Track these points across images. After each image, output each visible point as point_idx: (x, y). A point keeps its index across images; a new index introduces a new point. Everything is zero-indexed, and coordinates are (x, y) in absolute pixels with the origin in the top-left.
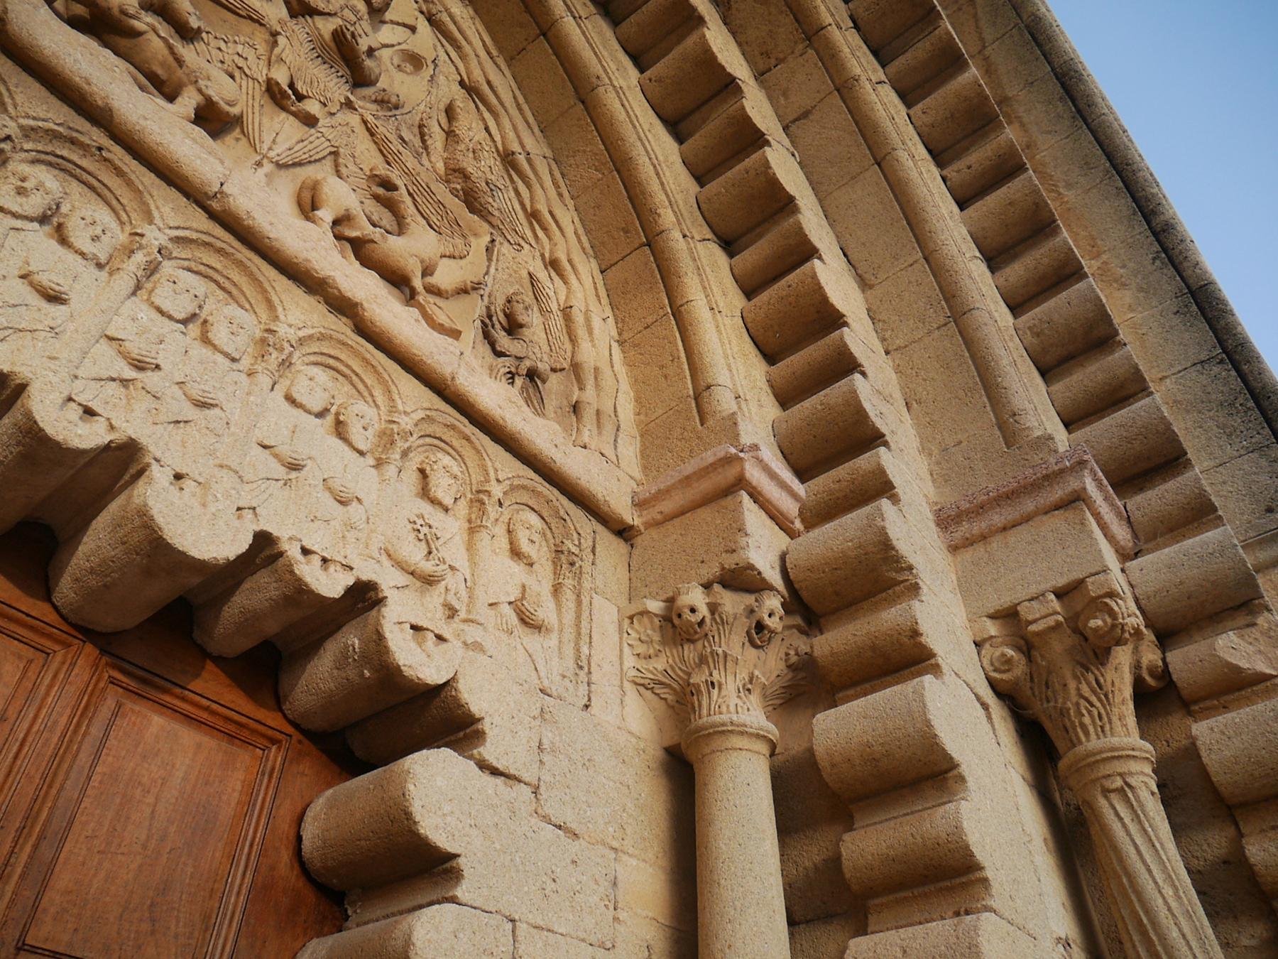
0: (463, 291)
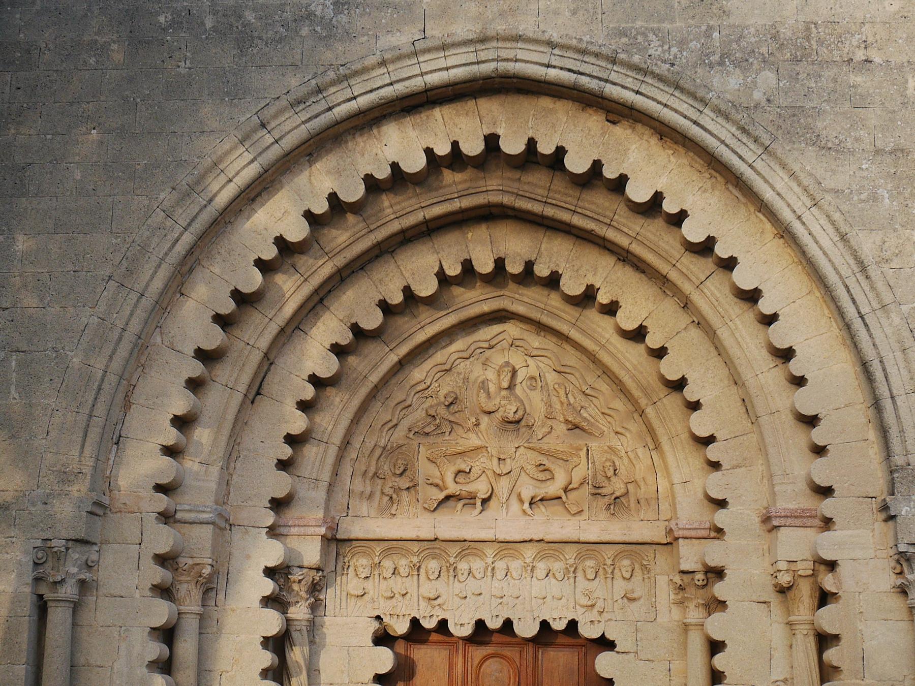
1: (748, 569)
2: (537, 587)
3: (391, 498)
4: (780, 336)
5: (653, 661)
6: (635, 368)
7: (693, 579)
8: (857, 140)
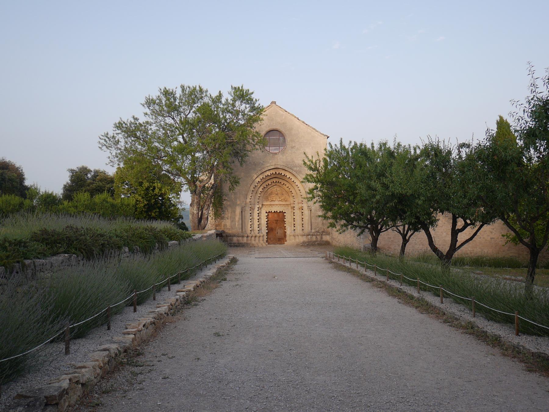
1: (297, 207)
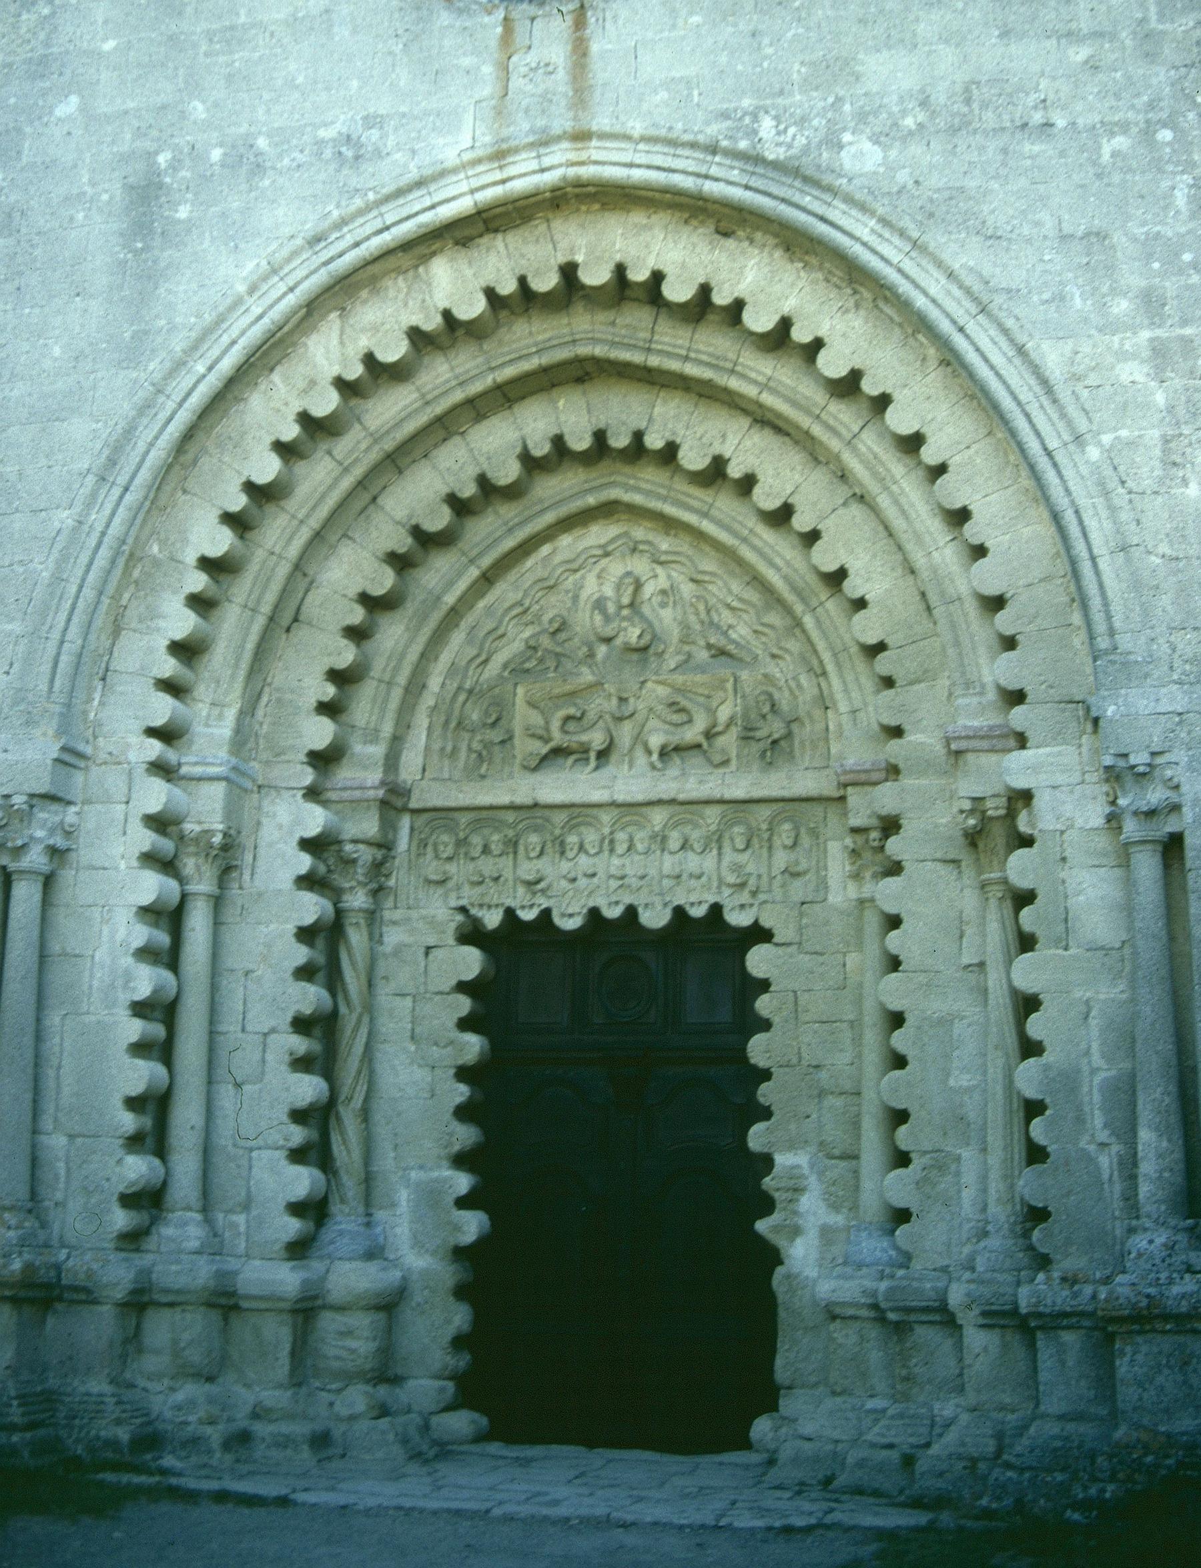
0: (728, 726)
2: (669, 864)
3: (480, 755)
4: (954, 491)
5: (822, 954)
6: (788, 563)
7: (867, 841)
8: (1038, 224)
